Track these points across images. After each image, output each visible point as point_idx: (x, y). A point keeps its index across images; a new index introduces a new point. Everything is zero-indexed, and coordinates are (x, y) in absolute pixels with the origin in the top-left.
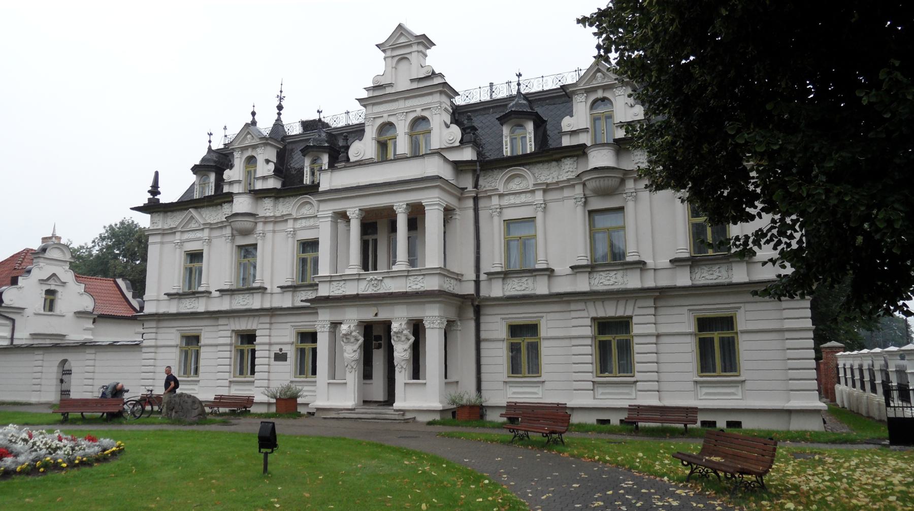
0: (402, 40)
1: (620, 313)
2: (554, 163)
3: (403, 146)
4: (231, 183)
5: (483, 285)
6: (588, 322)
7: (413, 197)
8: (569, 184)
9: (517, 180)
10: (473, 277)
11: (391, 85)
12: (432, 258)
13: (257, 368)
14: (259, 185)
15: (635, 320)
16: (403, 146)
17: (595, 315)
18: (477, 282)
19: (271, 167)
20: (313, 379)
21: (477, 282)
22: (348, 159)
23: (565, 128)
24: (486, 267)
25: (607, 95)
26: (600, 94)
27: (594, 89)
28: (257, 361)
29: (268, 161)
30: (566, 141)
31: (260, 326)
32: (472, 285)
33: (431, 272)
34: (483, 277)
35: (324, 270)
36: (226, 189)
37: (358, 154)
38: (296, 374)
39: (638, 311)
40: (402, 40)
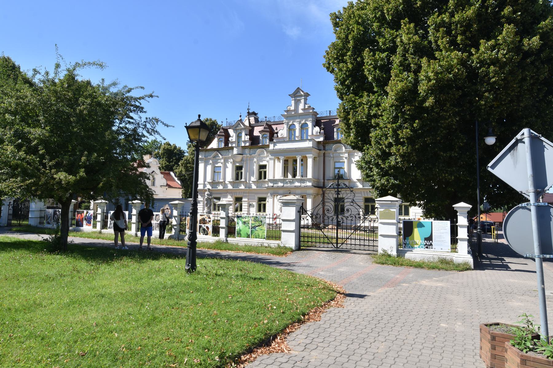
0: (298, 94)
3: (297, 133)
4: (232, 143)
5: (326, 183)
6: (362, 198)
10: (322, 181)
12: (310, 175)
13: (243, 210)
14: (243, 145)
16: (297, 133)
17: (363, 196)
18: (324, 183)
19: (248, 137)
21: (324, 183)
24: (326, 178)
28: (243, 207)
29: (246, 135)
31: (245, 195)
32: (322, 184)
33: (309, 180)
34: (326, 181)
35: (270, 176)
36: (230, 145)
37: (282, 134)
40: (298, 94)
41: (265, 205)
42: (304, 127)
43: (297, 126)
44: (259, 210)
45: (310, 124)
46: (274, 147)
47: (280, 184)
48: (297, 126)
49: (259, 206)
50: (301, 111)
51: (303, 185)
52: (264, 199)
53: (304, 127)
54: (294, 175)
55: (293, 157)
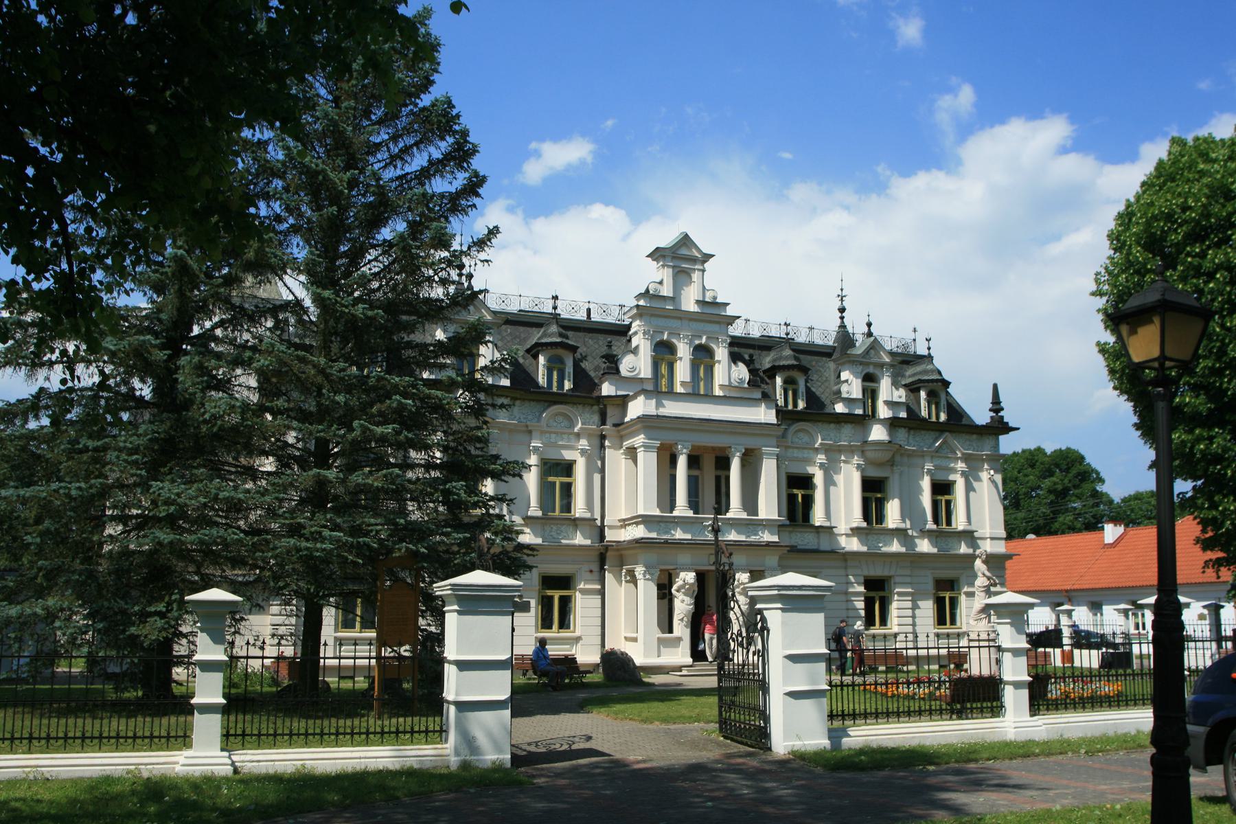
1: (886, 573)
2: (832, 426)
3: (682, 371)
7: (751, 442)
8: (850, 451)
9: (801, 435)
11: (673, 299)
15: (897, 579)
16: (682, 371)
17: (866, 573)
20: (564, 634)
22: (618, 371)
23: (844, 395)
25: (877, 372)
26: (871, 370)
27: (868, 364)
30: (840, 408)
37: (633, 369)
38: (336, 625)
39: (900, 572)
40: (684, 251)
41: (566, 603)
42: (703, 355)
43: (684, 351)
44: (546, 623)
45: (721, 353)
46: (657, 408)
47: (679, 534)
48: (684, 351)
49: (546, 603)
50: (693, 308)
51: (753, 538)
52: (565, 582)
53: (703, 355)
54: (721, 504)
55: (713, 449)
